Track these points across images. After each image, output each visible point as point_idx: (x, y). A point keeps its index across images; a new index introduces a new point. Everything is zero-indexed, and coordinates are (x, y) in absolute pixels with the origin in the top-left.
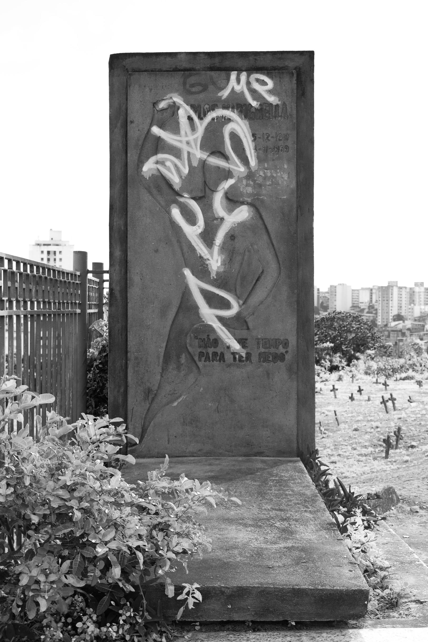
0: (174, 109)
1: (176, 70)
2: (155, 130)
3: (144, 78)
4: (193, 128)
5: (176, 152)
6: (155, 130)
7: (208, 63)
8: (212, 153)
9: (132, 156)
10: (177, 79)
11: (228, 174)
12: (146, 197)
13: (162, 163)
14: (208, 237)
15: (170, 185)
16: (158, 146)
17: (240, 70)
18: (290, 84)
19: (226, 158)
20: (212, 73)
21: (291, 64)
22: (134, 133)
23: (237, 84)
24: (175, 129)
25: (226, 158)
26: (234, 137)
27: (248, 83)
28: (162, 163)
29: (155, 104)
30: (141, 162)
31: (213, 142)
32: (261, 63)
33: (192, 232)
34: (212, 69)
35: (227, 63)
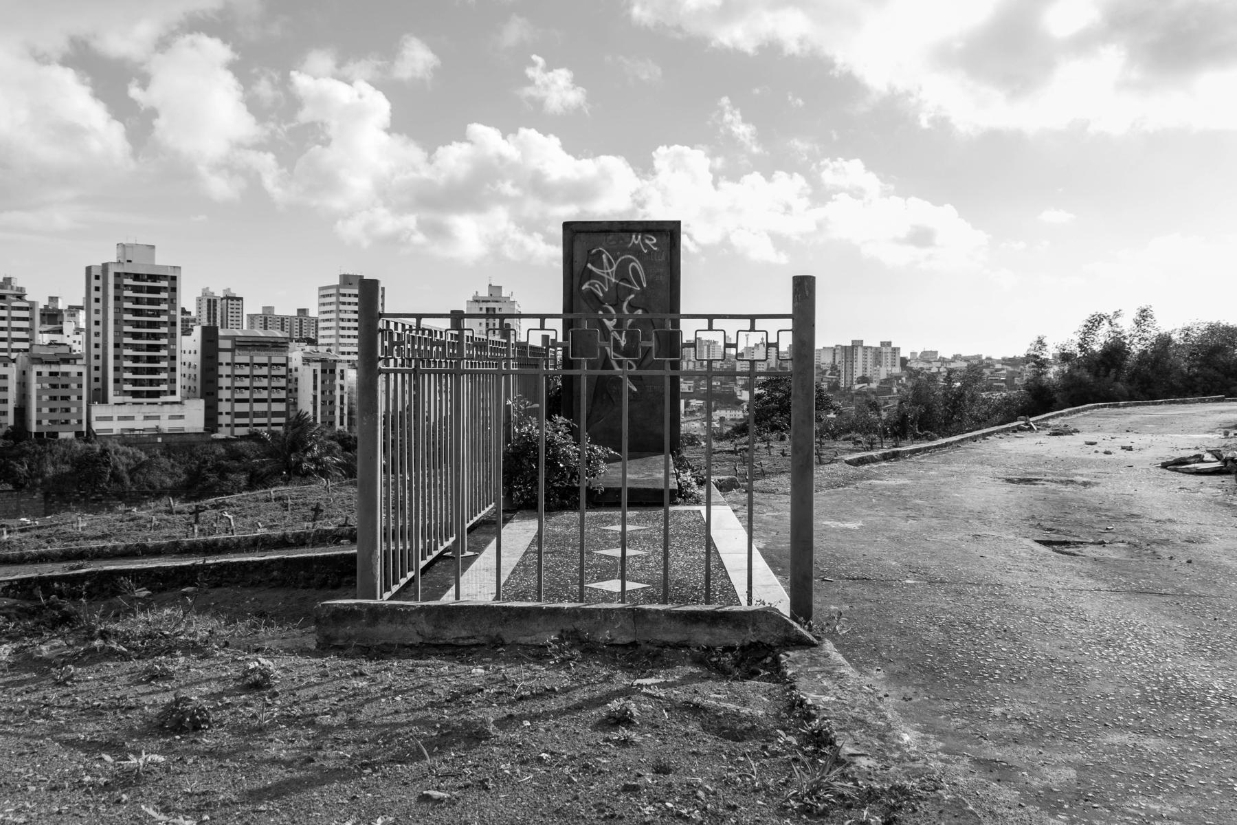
0: (600, 253)
1: (601, 232)
2: (589, 266)
3: (582, 236)
4: (611, 266)
5: (601, 279)
6: (589, 266)
7: (620, 226)
8: (621, 280)
9: (576, 280)
10: (602, 237)
11: (630, 291)
12: (584, 305)
13: (593, 285)
14: (619, 326)
15: (597, 296)
16: (590, 275)
17: (637, 232)
18: (667, 240)
19: (630, 282)
20: (623, 235)
21: (668, 228)
22: (577, 268)
23: (636, 240)
24: (601, 267)
25: (630, 282)
26: (634, 269)
27: (642, 240)
28: (593, 285)
29: (589, 251)
30: (582, 285)
31: (622, 274)
32: (650, 227)
33: (610, 324)
34: (622, 231)
35: (631, 227)
